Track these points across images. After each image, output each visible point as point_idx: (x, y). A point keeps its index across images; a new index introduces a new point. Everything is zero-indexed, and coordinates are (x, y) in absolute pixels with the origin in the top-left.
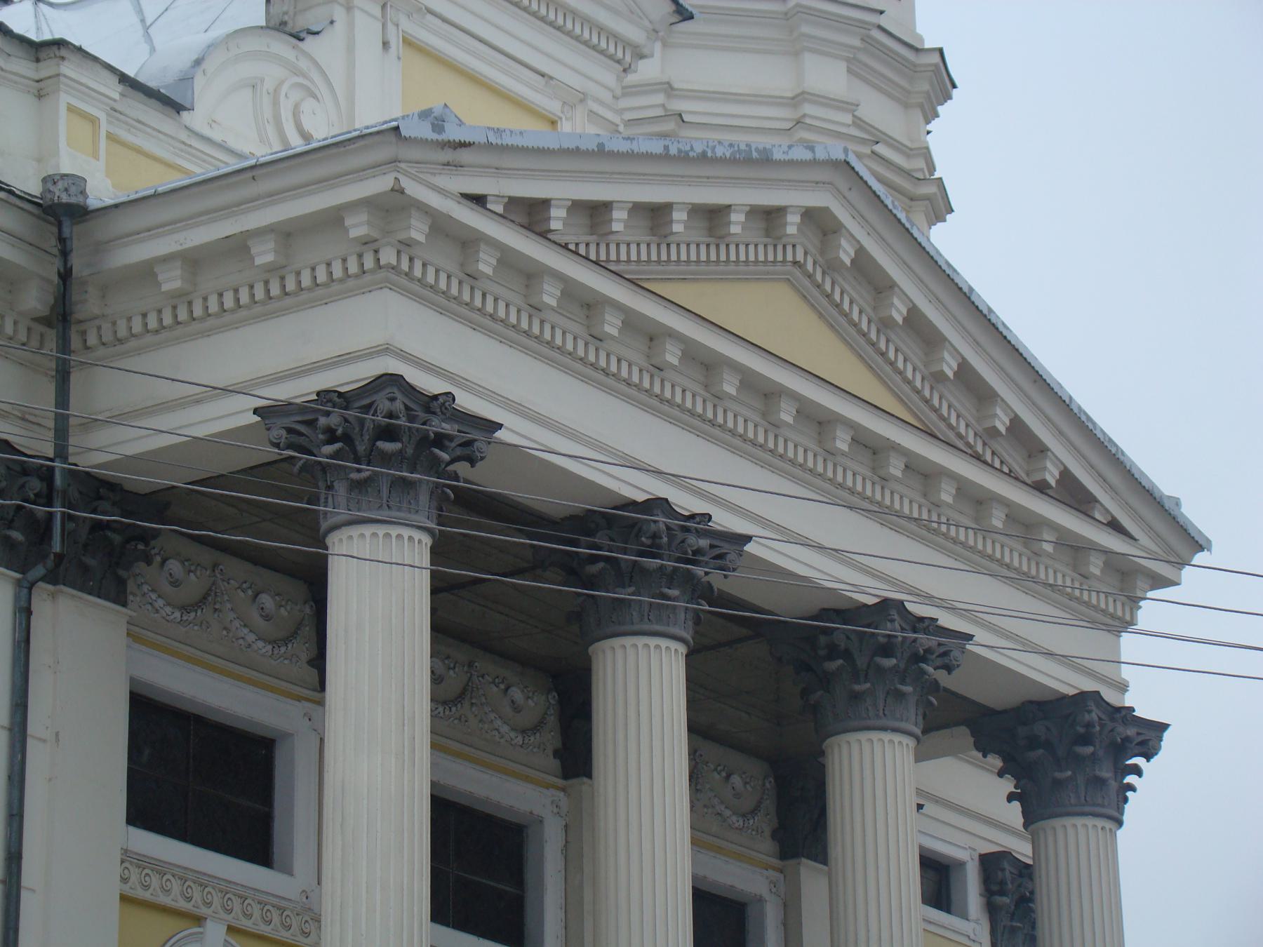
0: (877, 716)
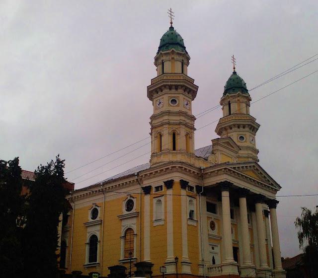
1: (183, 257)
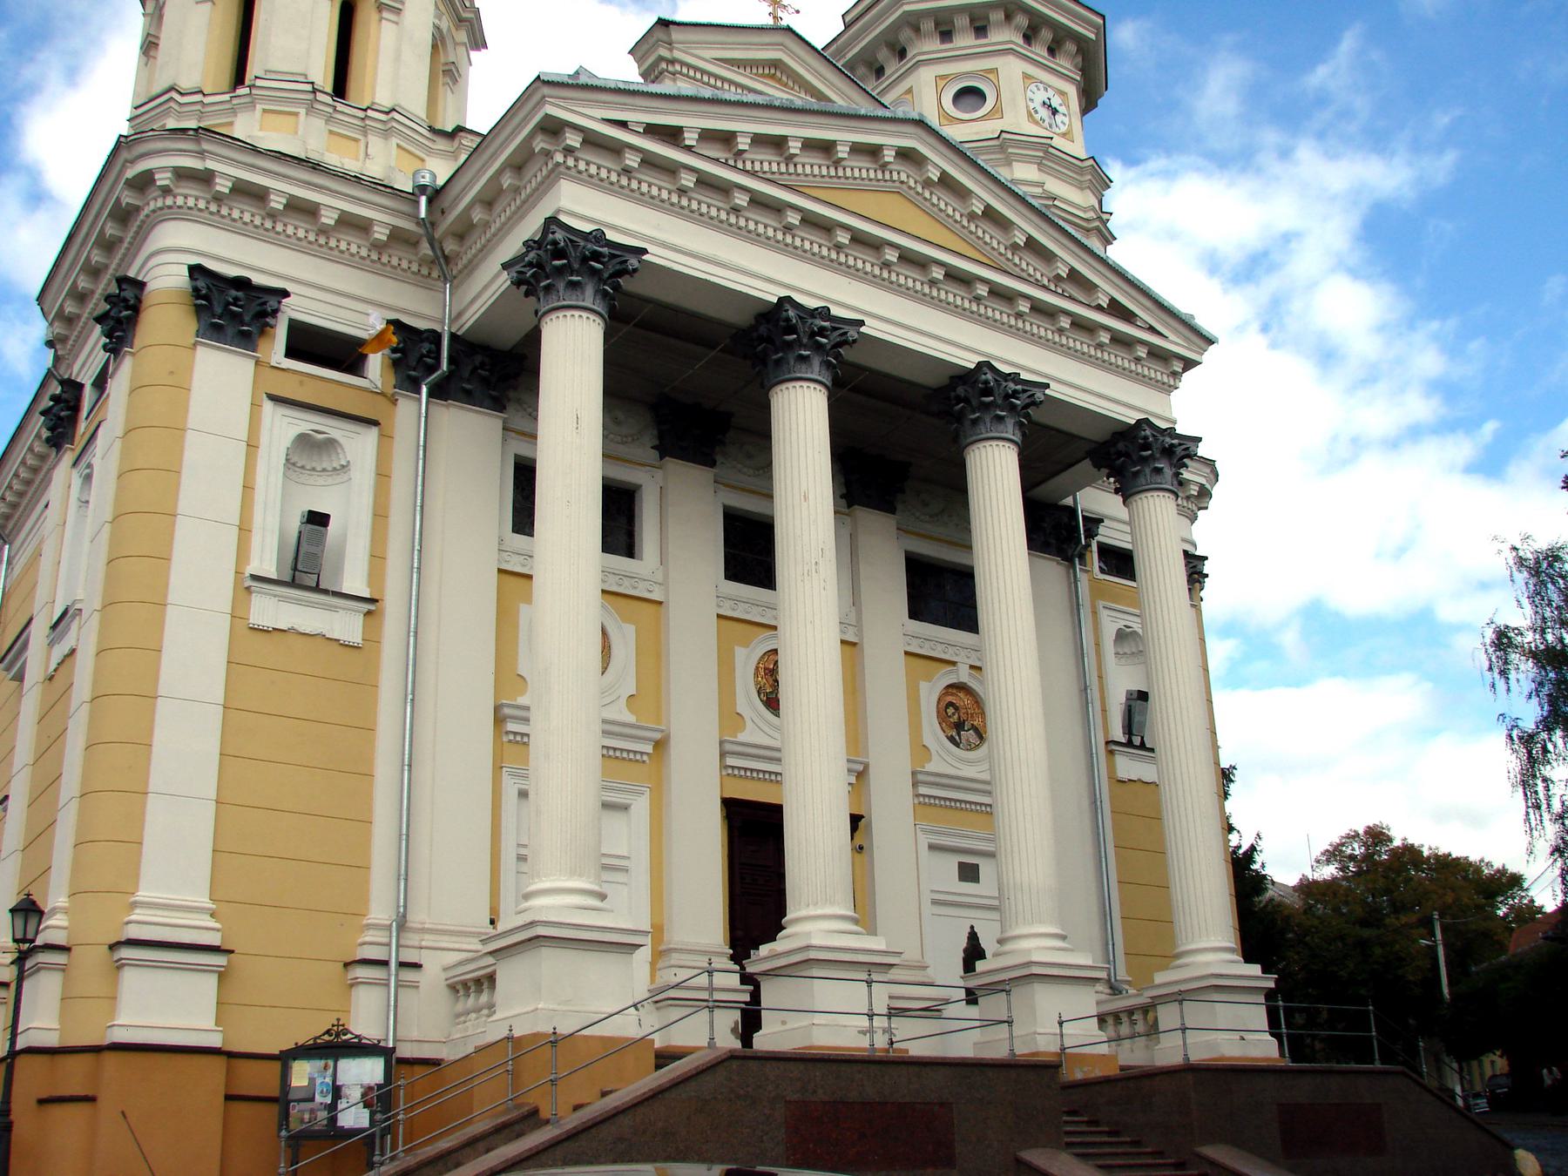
0: (987, 432)
1: (143, 894)
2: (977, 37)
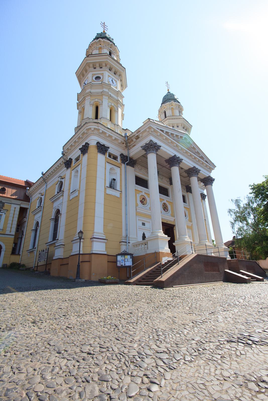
2: (177, 127)
